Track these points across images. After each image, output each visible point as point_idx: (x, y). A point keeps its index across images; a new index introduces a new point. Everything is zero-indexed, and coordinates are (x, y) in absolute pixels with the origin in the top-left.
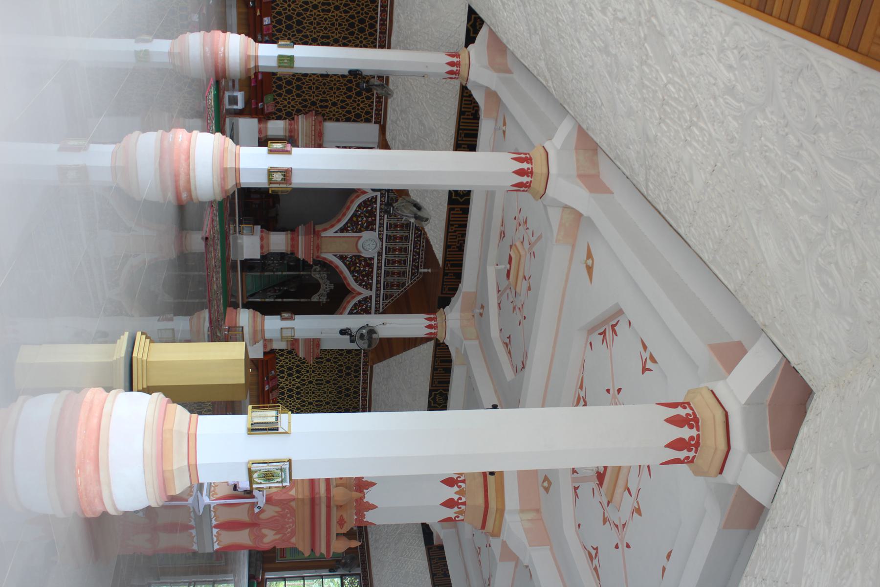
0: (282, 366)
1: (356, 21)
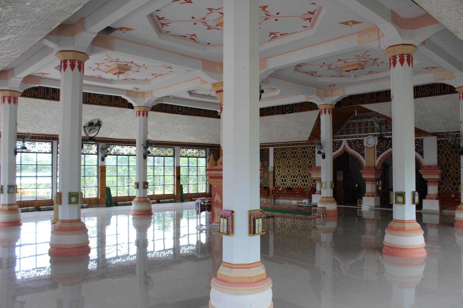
0: (302, 185)
1: (282, 155)
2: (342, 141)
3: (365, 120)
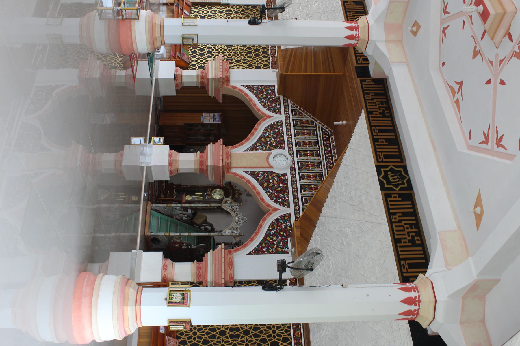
2: (280, 114)
3: (322, 152)
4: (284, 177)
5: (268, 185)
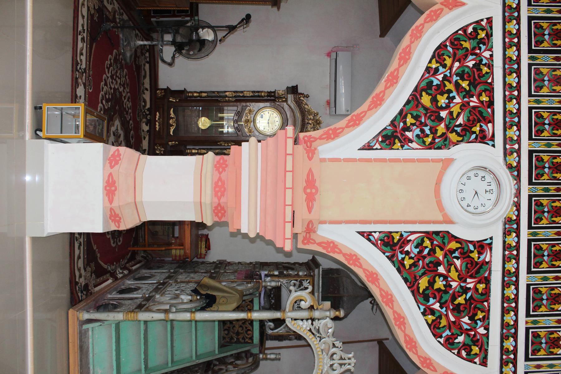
4: (480, 253)
5: (432, 283)
